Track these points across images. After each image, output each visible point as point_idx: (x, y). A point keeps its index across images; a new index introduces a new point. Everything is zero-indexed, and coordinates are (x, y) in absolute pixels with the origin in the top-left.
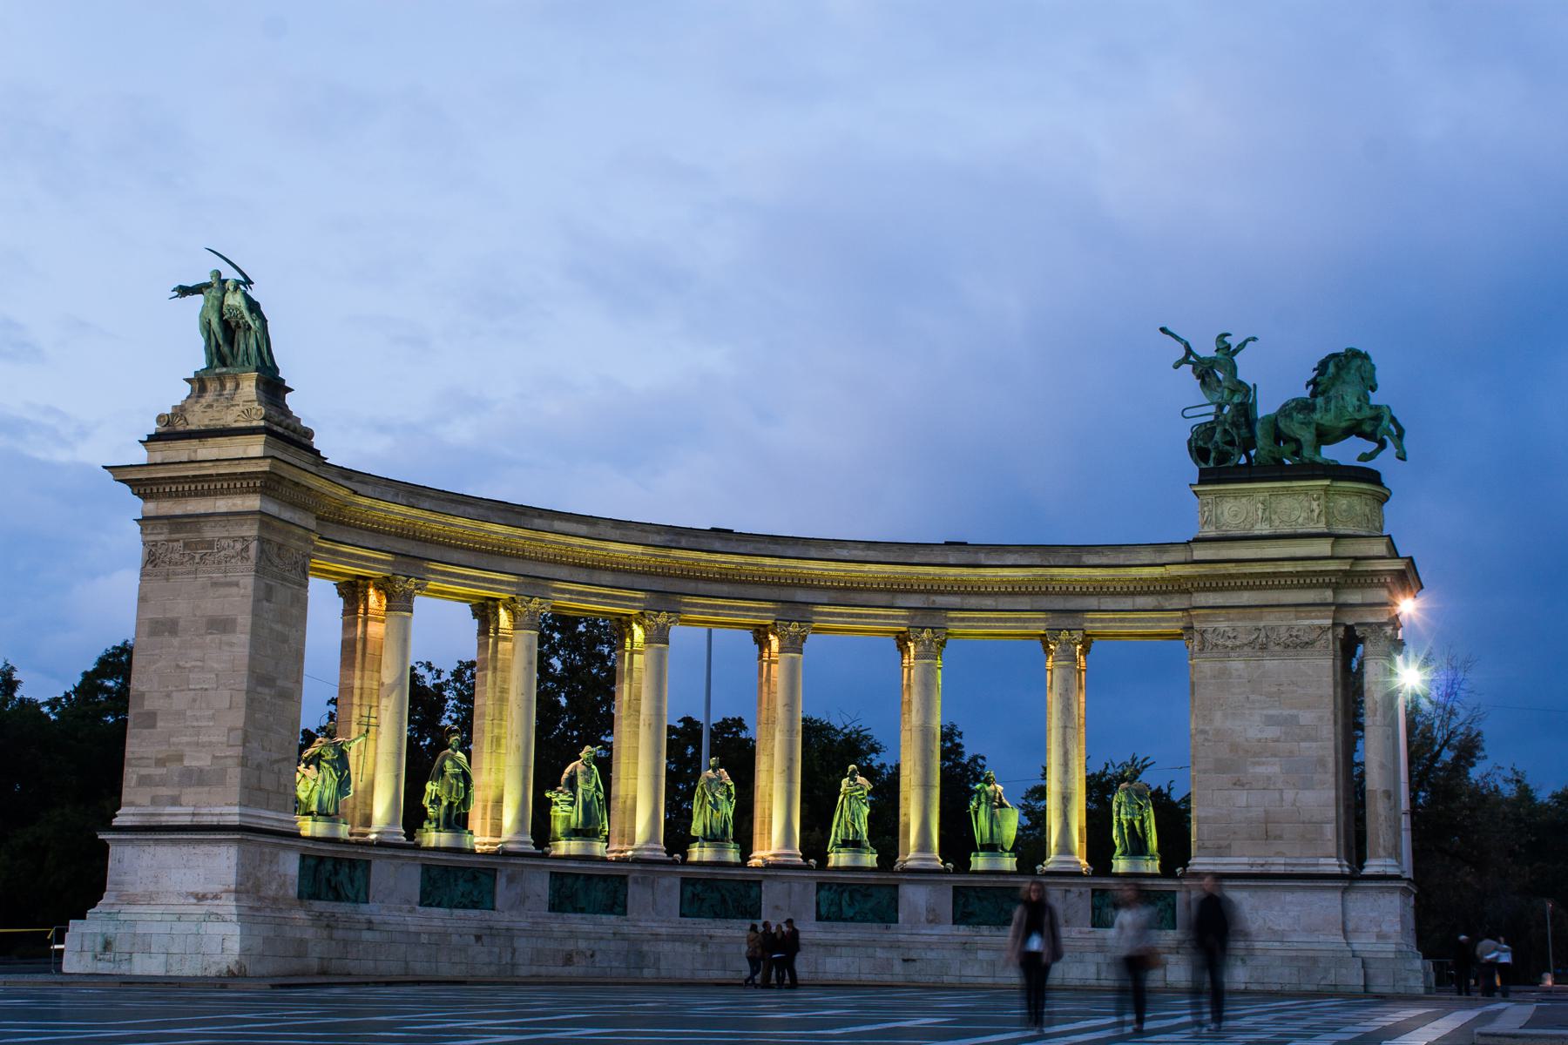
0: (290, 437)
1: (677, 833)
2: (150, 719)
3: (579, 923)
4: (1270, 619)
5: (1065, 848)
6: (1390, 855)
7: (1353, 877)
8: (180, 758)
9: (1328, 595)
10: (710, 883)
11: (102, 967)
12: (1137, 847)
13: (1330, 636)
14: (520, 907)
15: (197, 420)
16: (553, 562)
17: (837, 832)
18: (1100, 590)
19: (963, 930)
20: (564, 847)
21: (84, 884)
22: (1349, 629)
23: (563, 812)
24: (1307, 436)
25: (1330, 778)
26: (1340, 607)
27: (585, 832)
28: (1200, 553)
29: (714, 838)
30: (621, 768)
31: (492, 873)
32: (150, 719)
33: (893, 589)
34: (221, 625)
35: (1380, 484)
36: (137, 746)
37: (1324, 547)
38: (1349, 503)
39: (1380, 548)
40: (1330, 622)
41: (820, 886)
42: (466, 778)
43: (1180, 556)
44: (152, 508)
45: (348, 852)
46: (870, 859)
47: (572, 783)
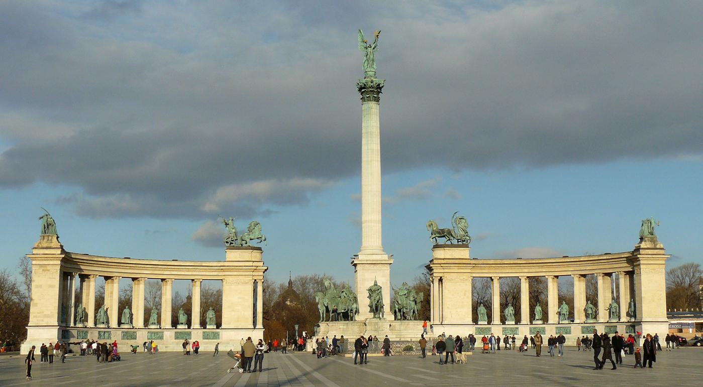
0: (62, 247)
2: (36, 305)
6: (260, 324)
7: (254, 328)
8: (43, 312)
9: (251, 273)
22: (255, 280)
26: (253, 276)
32: (36, 305)
34: (52, 286)
35: (261, 250)
36: (33, 310)
37: (251, 264)
39: (261, 264)
40: (251, 279)
41: (148, 332)
44: (34, 262)
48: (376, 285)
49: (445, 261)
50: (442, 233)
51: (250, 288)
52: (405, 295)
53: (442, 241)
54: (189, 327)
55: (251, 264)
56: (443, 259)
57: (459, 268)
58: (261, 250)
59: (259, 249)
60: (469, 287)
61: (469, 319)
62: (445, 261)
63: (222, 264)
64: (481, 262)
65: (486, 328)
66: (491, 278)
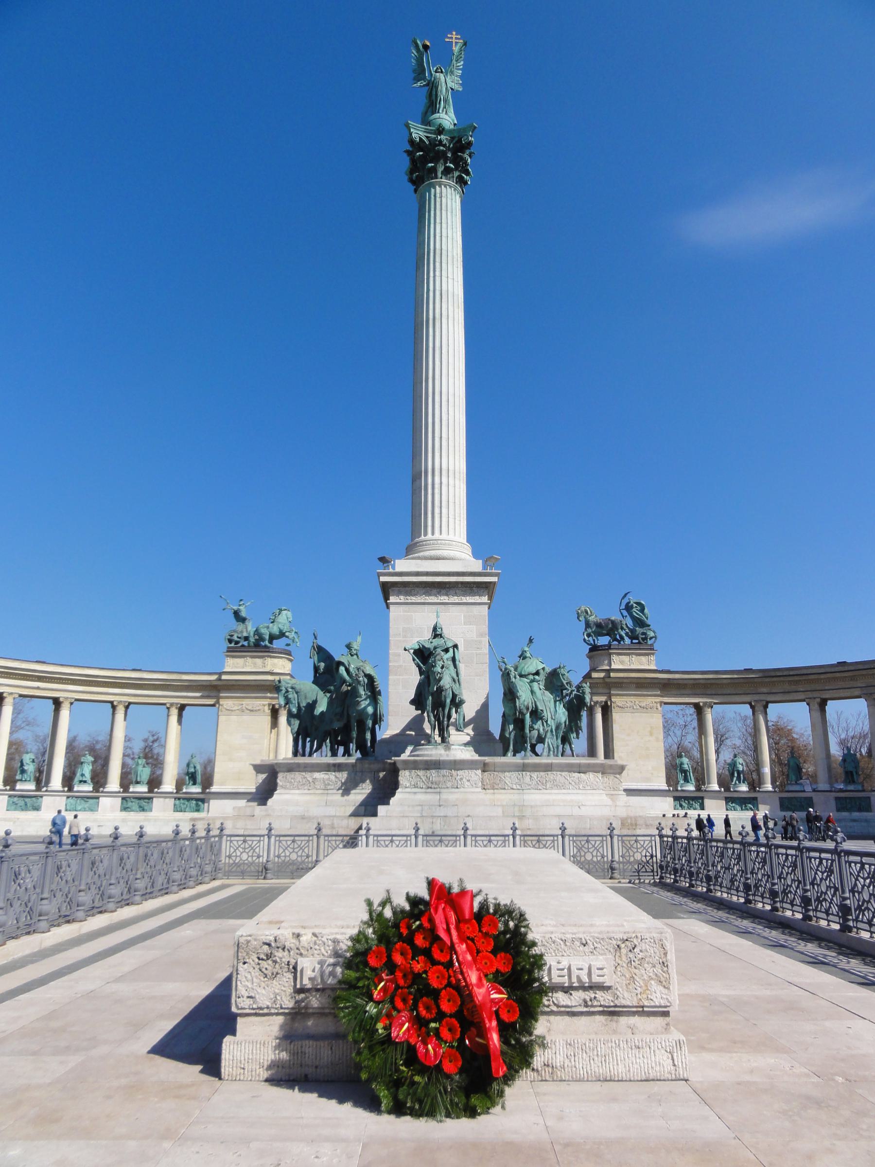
13: (266, 708)
17: (78, 777)
19: (124, 814)
22: (274, 706)
48: (436, 633)
49: (612, 675)
50: (608, 628)
52: (537, 673)
53: (604, 640)
54: (151, 791)
56: (608, 671)
58: (290, 655)
59: (289, 653)
61: (661, 784)
63: (214, 677)
64: (677, 676)
65: (694, 799)
66: (697, 706)
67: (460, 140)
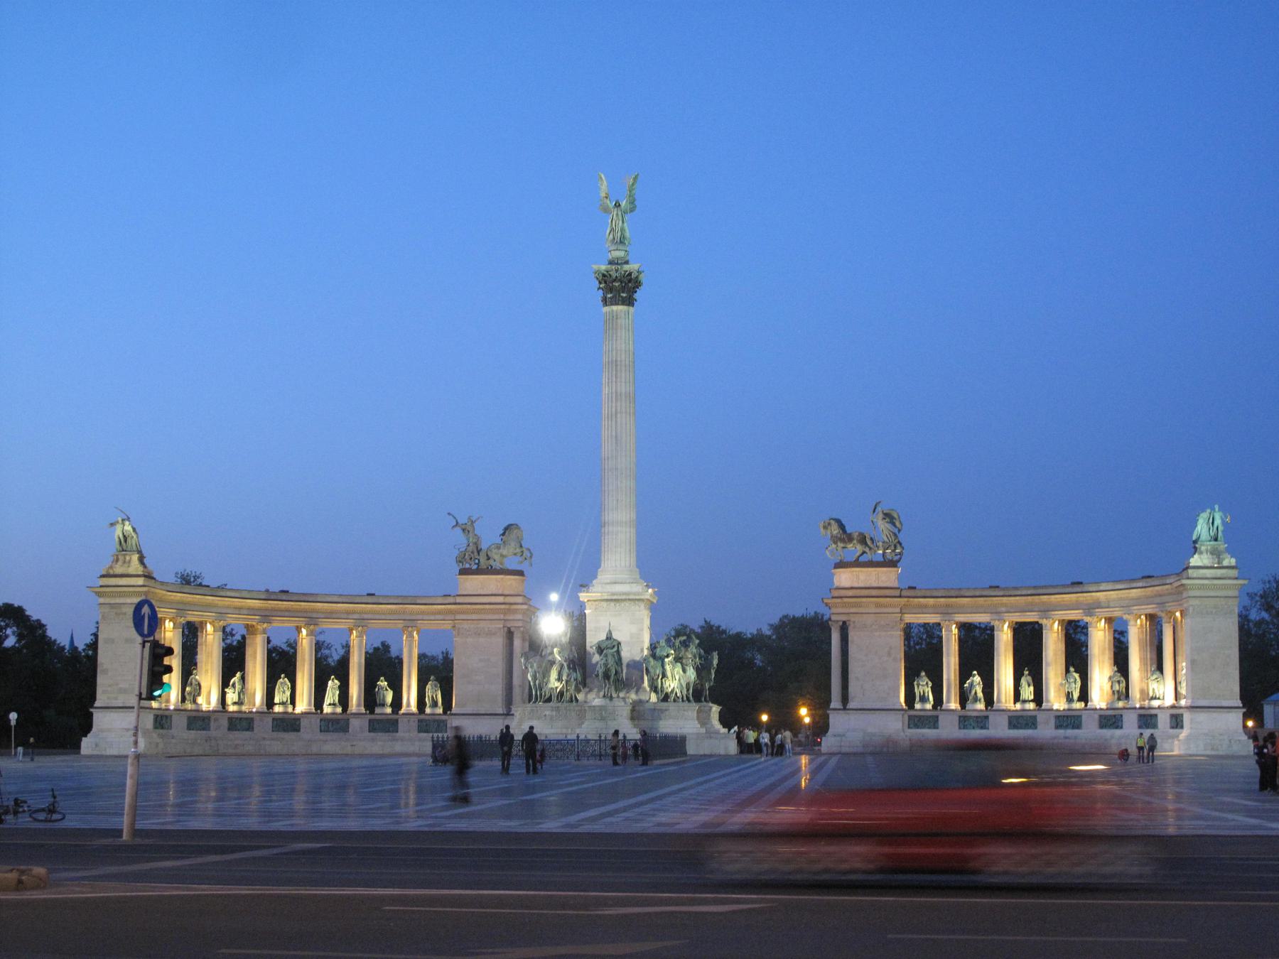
0: (148, 576)
1: (270, 701)
2: (105, 672)
3: (237, 734)
4: (482, 624)
5: (408, 705)
10: (282, 720)
11: (95, 753)
12: (435, 704)
14: (219, 729)
15: (119, 569)
16: (228, 607)
18: (423, 613)
20: (232, 708)
21: (86, 727)
23: (231, 696)
24: (496, 557)
25: (500, 680)
27: (239, 703)
28: (459, 600)
29: (283, 703)
30: (249, 678)
31: (209, 718)
32: (105, 672)
33: (348, 613)
36: (100, 680)
37: (500, 599)
38: (511, 581)
42: (199, 685)
43: (451, 600)
44: (102, 600)
45: (167, 713)
46: (339, 710)
47: (234, 685)
48: (609, 637)
51: (499, 641)
55: (500, 599)
57: (878, 605)
60: (896, 641)
62: (850, 593)
67: (630, 274)
